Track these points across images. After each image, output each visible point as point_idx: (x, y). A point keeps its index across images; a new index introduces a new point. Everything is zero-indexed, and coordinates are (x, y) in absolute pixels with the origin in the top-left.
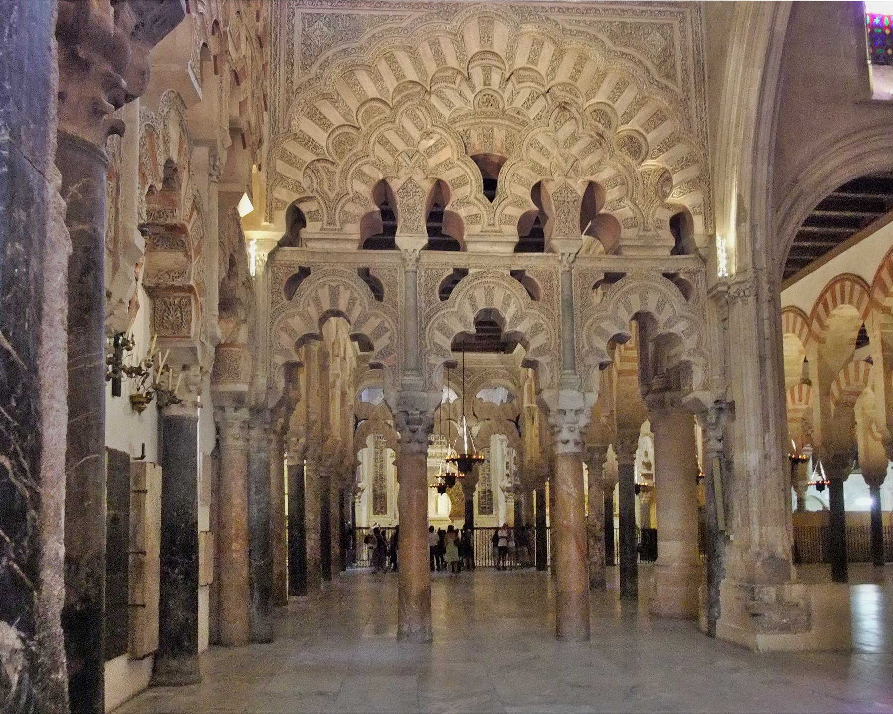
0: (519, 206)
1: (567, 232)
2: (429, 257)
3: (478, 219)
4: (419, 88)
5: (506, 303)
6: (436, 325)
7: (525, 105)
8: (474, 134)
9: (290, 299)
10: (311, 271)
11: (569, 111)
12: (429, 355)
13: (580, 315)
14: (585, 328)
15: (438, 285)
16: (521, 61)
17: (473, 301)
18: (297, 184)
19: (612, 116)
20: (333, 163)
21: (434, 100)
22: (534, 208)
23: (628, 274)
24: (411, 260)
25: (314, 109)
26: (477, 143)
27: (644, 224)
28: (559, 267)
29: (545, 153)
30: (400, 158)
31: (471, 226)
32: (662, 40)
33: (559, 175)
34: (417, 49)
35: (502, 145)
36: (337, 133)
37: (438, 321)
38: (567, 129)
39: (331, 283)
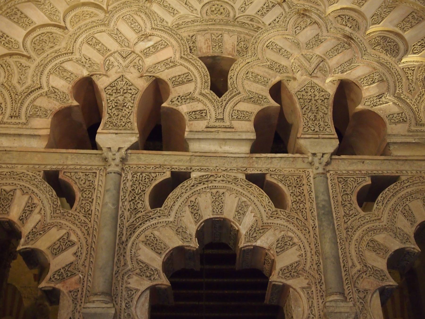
0: (254, 102)
1: (317, 129)
2: (139, 159)
3: (204, 114)
6: (142, 238)
7: (260, 13)
11: (310, 17)
12: (129, 277)
13: (344, 226)
14: (353, 242)
15: (149, 191)
19: (360, 20)
20: (29, 58)
22: (273, 103)
23: (403, 178)
24: (114, 160)
25: (15, 10)
26: (204, 47)
27: (415, 119)
28: (310, 170)
29: (286, 54)
30: (112, 59)
31: (195, 123)
33: (302, 75)
35: (233, 49)
36: (39, 32)
37: (148, 233)
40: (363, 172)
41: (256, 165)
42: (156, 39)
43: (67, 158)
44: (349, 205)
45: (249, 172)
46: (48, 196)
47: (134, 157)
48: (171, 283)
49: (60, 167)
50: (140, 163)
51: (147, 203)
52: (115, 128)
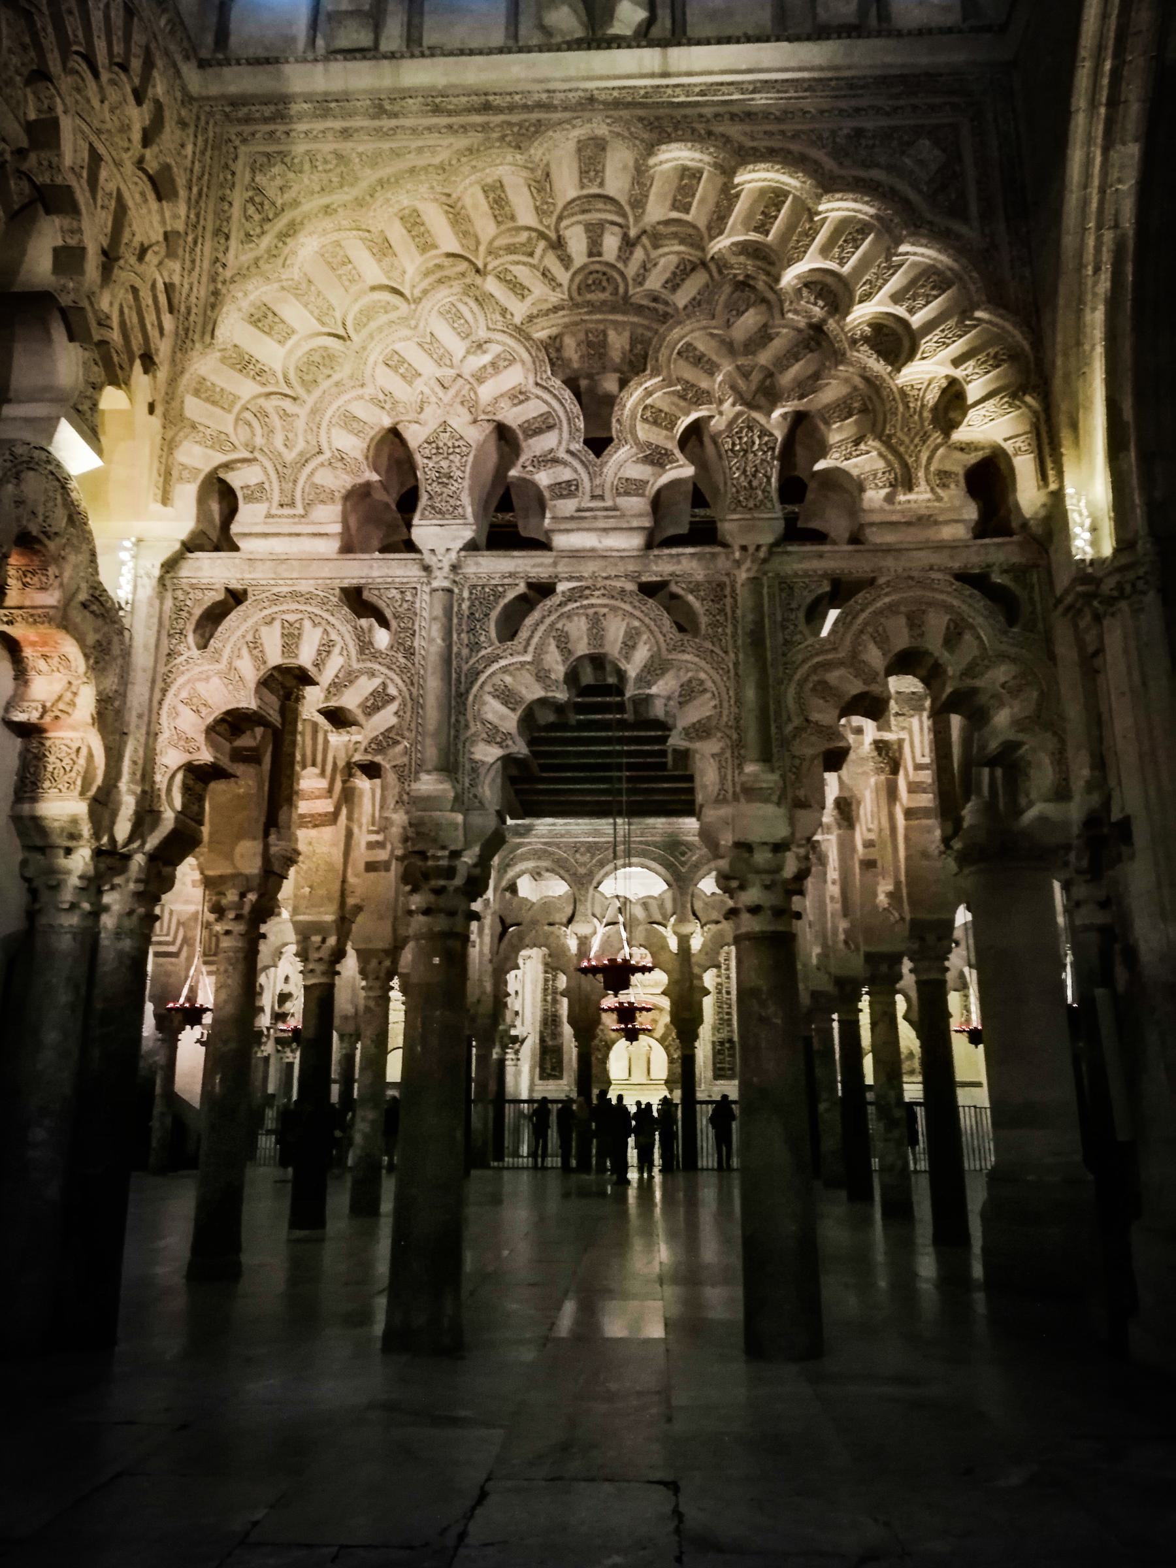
0: (652, 463)
3: (573, 488)
4: (463, 266)
5: (629, 645)
7: (668, 286)
8: (569, 342)
9: (203, 646)
10: (250, 594)
15: (494, 614)
16: (657, 211)
17: (563, 643)
18: (223, 437)
20: (295, 399)
21: (491, 285)
23: (882, 580)
28: (736, 572)
32: (937, 152)
33: (734, 405)
34: (459, 199)
35: (623, 359)
37: (496, 680)
38: (750, 320)
39: (286, 617)
40: (820, 572)
41: (654, 568)
42: (494, 349)
43: (371, 567)
44: (792, 627)
45: (644, 579)
46: (351, 629)
47: (470, 561)
48: (531, 751)
49: (363, 581)
50: (480, 570)
51: (493, 634)
52: (439, 516)
